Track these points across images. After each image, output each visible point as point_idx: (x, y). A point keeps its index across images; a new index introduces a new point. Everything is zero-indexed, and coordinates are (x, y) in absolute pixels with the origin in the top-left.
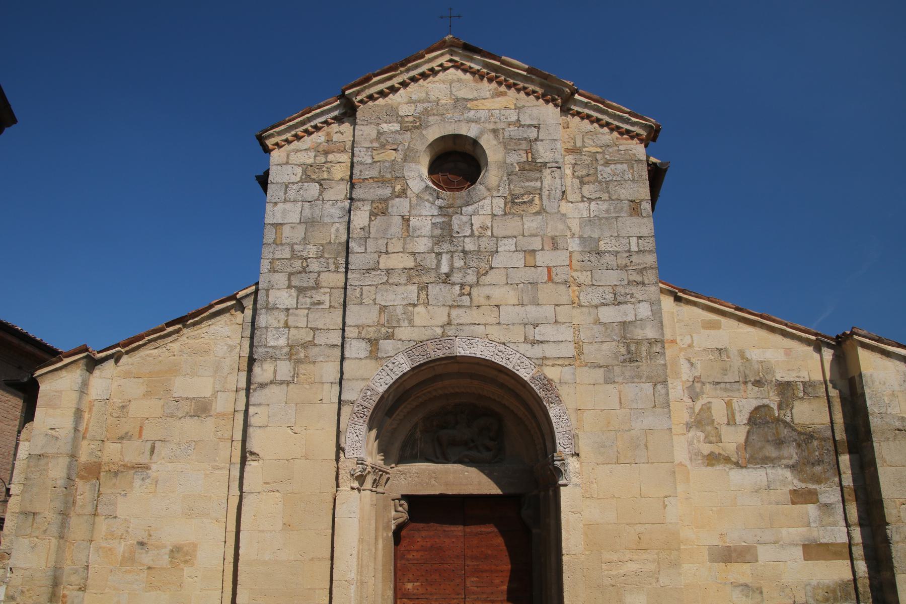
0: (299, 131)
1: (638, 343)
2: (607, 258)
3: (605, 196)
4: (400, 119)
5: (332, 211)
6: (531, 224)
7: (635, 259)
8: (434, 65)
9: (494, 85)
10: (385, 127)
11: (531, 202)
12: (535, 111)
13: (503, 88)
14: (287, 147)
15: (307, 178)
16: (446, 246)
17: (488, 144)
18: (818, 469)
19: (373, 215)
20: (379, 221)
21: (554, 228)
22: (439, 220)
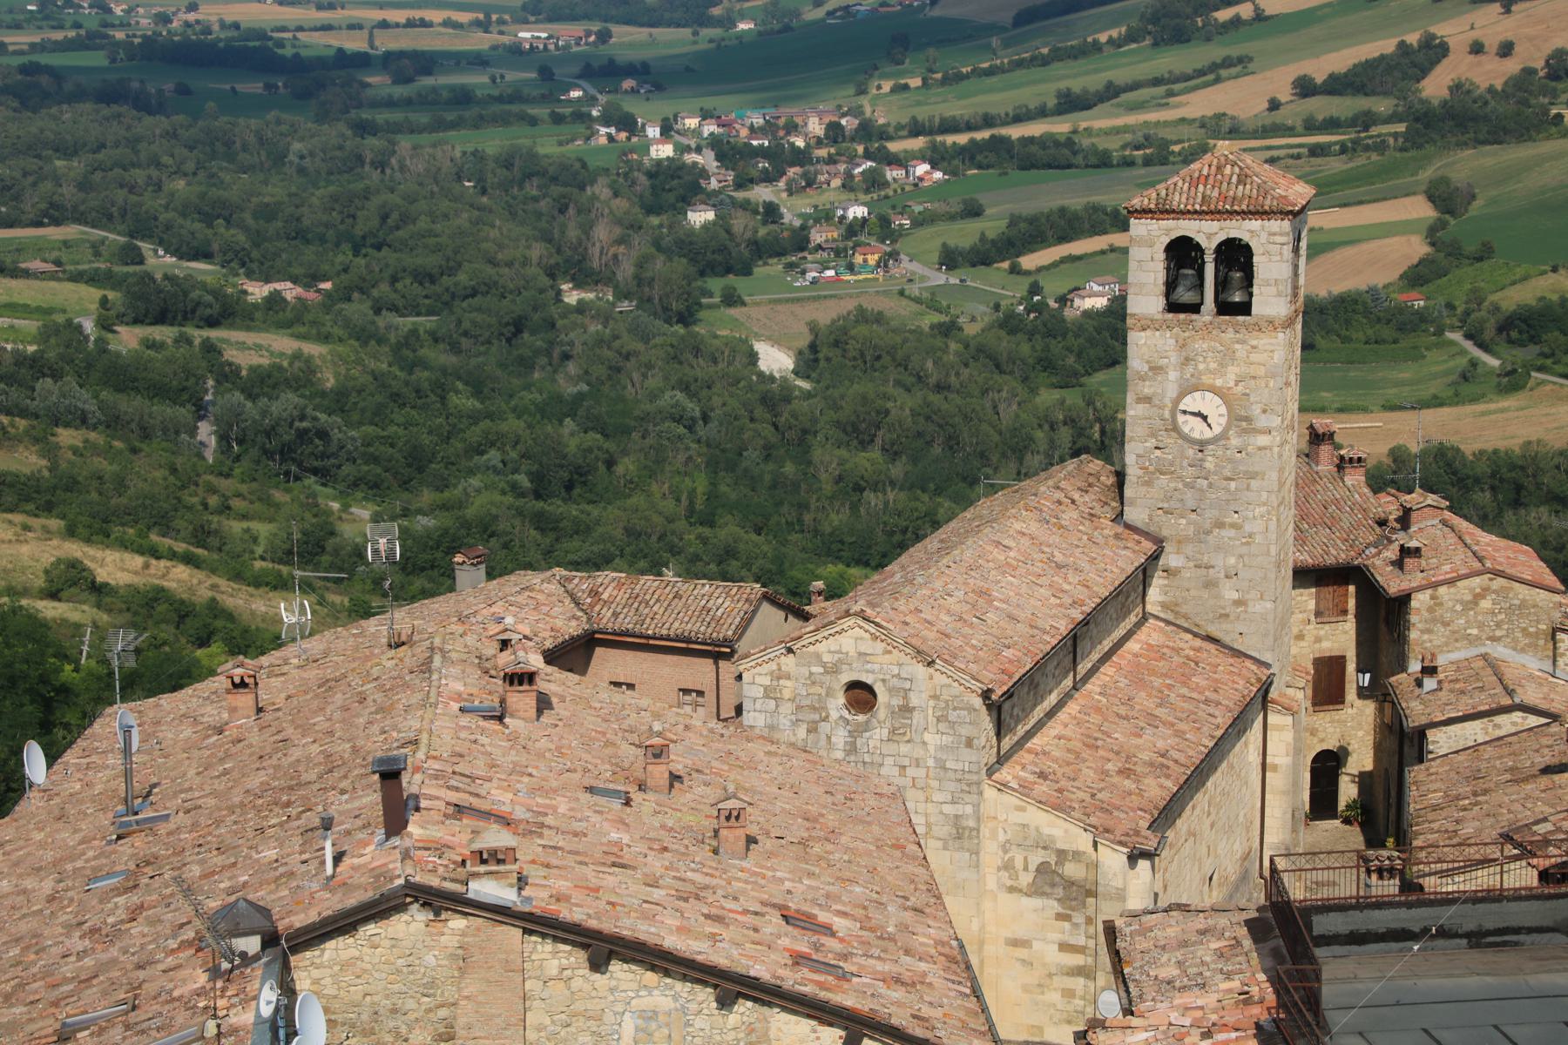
0: (760, 661)
1: (964, 828)
2: (951, 775)
3: (951, 732)
4: (824, 665)
5: (785, 721)
6: (904, 748)
7: (967, 776)
8: (845, 626)
9: (884, 645)
10: (817, 669)
11: (904, 734)
12: (910, 669)
13: (890, 648)
14: (753, 671)
15: (767, 696)
16: (852, 758)
17: (879, 689)
18: (1074, 903)
19: (809, 731)
20: (811, 736)
21: (918, 752)
22: (849, 739)
